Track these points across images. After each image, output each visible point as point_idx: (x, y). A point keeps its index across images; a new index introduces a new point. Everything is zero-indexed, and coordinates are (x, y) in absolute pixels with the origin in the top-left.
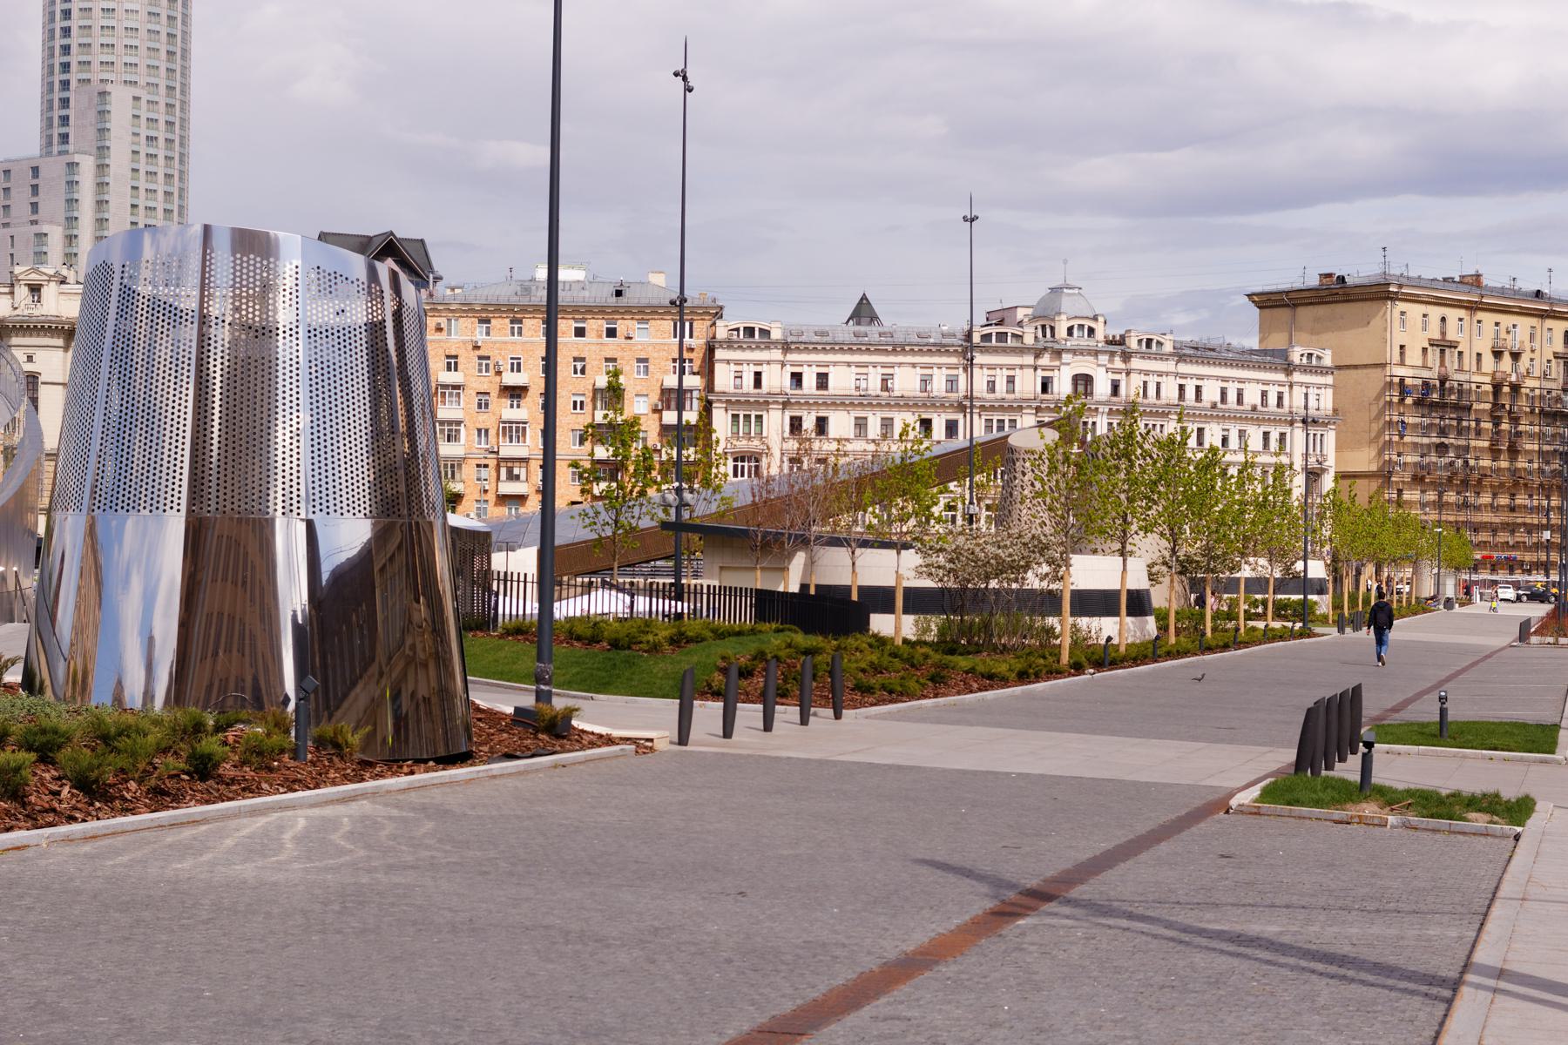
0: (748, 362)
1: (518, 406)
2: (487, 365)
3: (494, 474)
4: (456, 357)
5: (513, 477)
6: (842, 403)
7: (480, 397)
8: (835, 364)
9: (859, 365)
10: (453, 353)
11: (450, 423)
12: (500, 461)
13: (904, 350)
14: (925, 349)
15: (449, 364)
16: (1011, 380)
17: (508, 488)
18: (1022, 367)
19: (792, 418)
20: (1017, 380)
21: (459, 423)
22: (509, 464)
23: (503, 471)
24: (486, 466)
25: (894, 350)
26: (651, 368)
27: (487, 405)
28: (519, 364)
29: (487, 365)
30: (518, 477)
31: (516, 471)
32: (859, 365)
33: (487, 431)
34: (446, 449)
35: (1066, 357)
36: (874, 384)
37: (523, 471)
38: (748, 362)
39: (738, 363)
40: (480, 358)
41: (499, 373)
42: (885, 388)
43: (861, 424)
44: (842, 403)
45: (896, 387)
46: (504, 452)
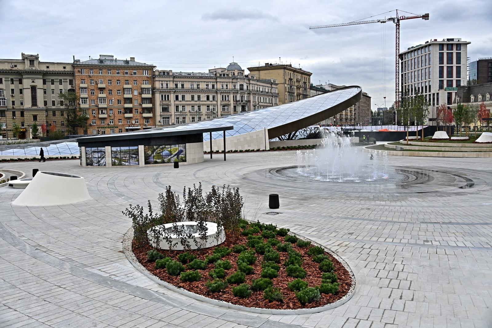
0: (165, 81)
1: (102, 93)
2: (93, 82)
3: (97, 112)
4: (84, 80)
5: (102, 113)
6: (188, 91)
7: (92, 91)
8: (186, 81)
9: (191, 82)
10: (83, 79)
11: (84, 98)
12: (99, 109)
13: (202, 78)
14: (205, 77)
15: (126, 83)
16: (227, 86)
17: (101, 116)
18: (170, 81)
19: (182, 96)
20: (228, 85)
21: (87, 98)
22: (102, 109)
23: (100, 111)
24: (94, 110)
25: (200, 78)
26: (138, 83)
27: (94, 94)
28: (102, 82)
29: (93, 82)
30: (104, 113)
31: (104, 112)
32: (191, 82)
33: (94, 101)
34: (83, 106)
35: (239, 80)
36: (195, 86)
37: (106, 111)
38: (165, 81)
39: (162, 81)
40: (91, 80)
41: (97, 84)
42: (198, 88)
43: (193, 97)
44: (188, 91)
45: (200, 87)
46: (100, 106)
